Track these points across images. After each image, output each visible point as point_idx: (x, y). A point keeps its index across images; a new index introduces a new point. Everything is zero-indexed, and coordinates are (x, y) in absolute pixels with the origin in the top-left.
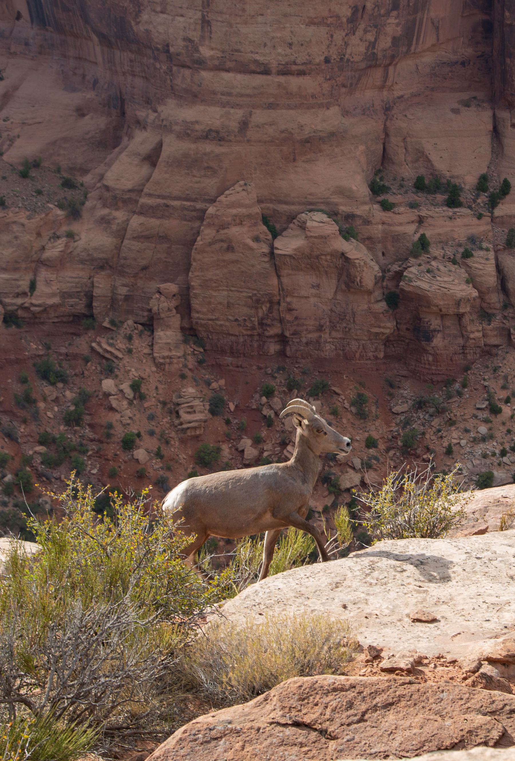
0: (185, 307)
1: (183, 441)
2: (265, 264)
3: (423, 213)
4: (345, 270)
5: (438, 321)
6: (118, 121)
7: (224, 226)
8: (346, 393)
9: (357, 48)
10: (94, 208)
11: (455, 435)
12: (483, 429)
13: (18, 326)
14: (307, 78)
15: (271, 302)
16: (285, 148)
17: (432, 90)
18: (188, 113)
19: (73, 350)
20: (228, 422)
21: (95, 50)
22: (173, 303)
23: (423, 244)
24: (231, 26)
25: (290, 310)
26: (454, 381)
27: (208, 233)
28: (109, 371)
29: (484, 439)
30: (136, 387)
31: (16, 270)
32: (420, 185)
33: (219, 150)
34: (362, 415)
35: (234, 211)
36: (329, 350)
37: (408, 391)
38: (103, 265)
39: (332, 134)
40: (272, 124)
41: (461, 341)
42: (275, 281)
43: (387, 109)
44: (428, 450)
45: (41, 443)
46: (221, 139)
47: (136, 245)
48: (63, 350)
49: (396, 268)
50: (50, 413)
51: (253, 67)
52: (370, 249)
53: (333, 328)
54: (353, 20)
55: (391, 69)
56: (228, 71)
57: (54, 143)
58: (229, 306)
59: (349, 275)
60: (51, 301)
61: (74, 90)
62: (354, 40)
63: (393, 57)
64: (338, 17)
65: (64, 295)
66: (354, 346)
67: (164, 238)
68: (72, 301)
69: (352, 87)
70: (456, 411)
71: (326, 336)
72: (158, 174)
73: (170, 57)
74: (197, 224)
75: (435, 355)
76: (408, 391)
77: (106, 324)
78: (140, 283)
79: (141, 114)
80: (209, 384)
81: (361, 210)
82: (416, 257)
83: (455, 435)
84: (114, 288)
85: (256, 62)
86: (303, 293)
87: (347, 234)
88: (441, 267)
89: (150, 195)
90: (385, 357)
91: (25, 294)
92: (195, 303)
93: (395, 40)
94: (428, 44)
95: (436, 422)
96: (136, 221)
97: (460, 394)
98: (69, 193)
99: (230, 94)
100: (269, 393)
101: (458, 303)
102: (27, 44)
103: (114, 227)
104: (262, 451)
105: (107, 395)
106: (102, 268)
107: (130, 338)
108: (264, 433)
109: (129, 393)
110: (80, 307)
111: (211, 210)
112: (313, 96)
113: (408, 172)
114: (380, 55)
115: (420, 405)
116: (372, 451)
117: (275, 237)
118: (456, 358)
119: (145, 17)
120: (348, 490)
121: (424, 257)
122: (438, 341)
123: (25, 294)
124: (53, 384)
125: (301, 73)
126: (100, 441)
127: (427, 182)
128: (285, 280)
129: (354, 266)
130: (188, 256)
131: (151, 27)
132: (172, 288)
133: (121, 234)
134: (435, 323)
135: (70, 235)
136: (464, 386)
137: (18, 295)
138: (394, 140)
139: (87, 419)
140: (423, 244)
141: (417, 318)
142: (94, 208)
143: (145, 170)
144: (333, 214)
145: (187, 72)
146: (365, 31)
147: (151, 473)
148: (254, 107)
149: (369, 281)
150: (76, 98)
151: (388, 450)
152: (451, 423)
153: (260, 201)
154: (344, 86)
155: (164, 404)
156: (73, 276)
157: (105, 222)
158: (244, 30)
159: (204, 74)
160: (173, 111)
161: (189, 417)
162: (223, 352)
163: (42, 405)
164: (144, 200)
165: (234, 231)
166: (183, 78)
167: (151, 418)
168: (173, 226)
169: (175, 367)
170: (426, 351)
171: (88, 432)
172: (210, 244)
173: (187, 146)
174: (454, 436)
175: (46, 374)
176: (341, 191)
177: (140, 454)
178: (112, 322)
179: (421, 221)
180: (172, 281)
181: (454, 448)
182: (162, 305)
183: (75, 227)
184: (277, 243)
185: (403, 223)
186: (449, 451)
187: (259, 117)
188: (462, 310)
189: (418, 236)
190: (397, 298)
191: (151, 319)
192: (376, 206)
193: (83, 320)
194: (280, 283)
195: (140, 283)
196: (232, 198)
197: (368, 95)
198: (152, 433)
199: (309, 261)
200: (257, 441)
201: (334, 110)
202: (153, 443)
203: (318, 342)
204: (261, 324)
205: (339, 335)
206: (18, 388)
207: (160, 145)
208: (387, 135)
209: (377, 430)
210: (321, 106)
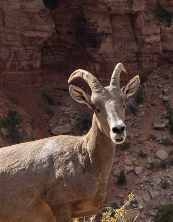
5: (107, 23)
12: (163, 153)
29: (164, 165)
41: (134, 47)
83: (128, 160)
90: (43, 66)
134: (103, 25)
141: (81, 20)
181: (128, 177)
188: (135, 9)
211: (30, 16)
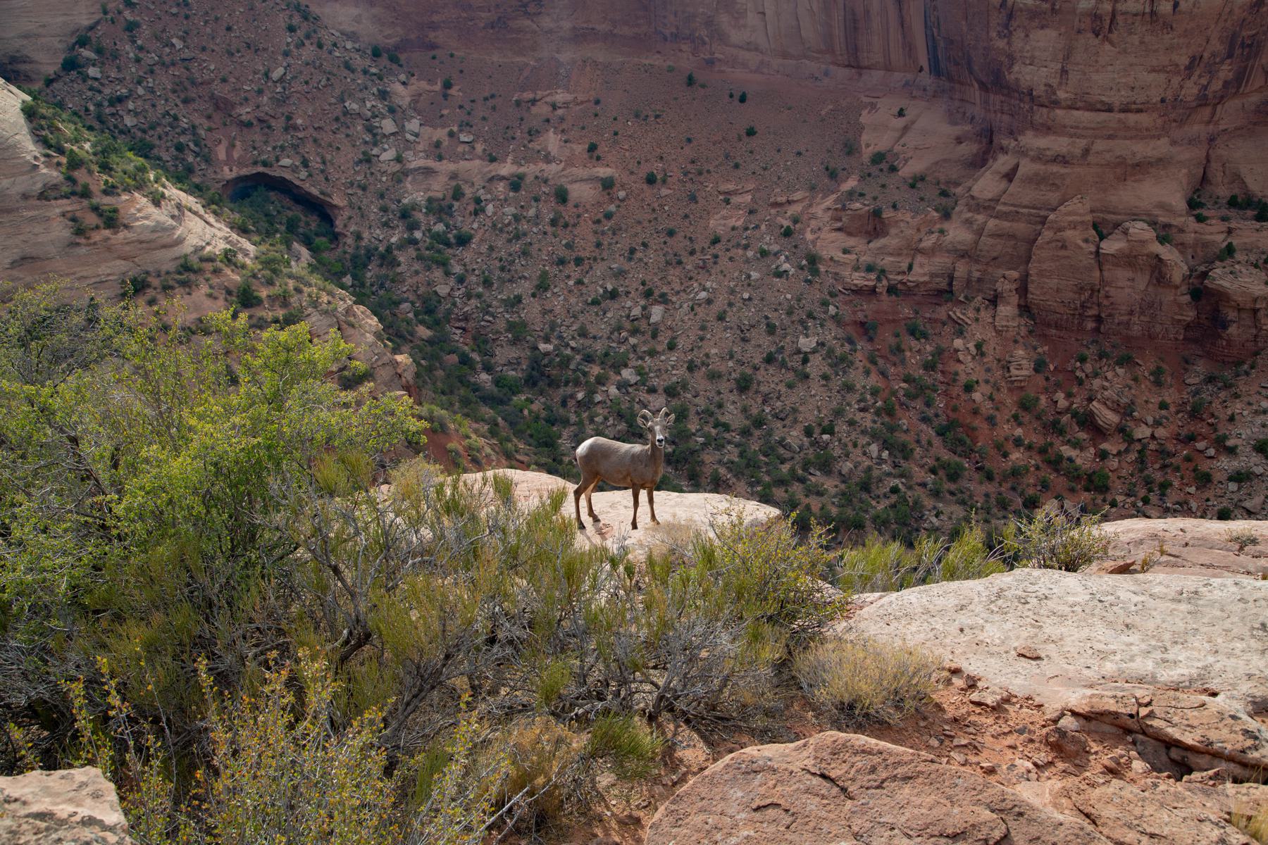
0: (1023, 290)
1: (1010, 390)
2: (1091, 260)
3: (1232, 226)
4: (1157, 268)
5: (1236, 314)
6: (988, 144)
7: (1060, 230)
8: (1147, 365)
9: (1191, 90)
10: (961, 212)
11: (1238, 406)
13: (897, 295)
14: (1144, 114)
15: (1092, 290)
16: (1118, 170)
17: (1255, 124)
18: (1042, 142)
19: (934, 316)
20: (1047, 379)
21: (975, 93)
22: (1014, 286)
23: (1230, 250)
24: (1085, 74)
25: (1107, 297)
26: (1244, 363)
27: (1047, 234)
28: (960, 333)
30: (978, 346)
31: (899, 255)
32: (1233, 203)
33: (1063, 171)
34: (1158, 383)
35: (1071, 218)
36: (1136, 330)
37: (1201, 368)
38: (964, 254)
39: (1160, 160)
40: (1109, 151)
41: (1254, 331)
42: (1097, 274)
43: (1211, 140)
44: (1213, 415)
45: (905, 381)
46: (1066, 162)
47: (991, 241)
48: (928, 315)
49: (1202, 268)
50: (913, 360)
51: (1099, 106)
52: (1181, 252)
53: (1142, 313)
54: (1190, 68)
55: (1219, 107)
56: (1077, 109)
57: (937, 163)
58: (1058, 290)
59: (1160, 272)
60: (922, 279)
61: (956, 124)
62: (1189, 84)
63: (1222, 97)
64: (1177, 65)
65: (933, 275)
66: (1158, 328)
67: (1012, 236)
68: (938, 280)
69: (1181, 122)
70: (1242, 386)
71: (1135, 319)
72: (1013, 188)
73: (1032, 99)
74: (1039, 227)
75: (1229, 341)
76: (1201, 368)
77: (961, 298)
78: (990, 270)
79: (1005, 142)
80: (1035, 349)
81: (1177, 221)
82: (1222, 261)
83: (1238, 406)
84: (970, 272)
85: (1102, 102)
86: (1120, 284)
87: (1162, 240)
88: (1244, 270)
89: (1005, 204)
91: (904, 273)
92: (1031, 287)
93: (1226, 84)
94: (1257, 85)
95: (1223, 395)
96: (992, 223)
97: (1247, 374)
98: (944, 201)
99: (1077, 127)
100: (1083, 360)
101: (1255, 300)
102: (925, 90)
103: (975, 227)
104: (1072, 403)
105: (957, 351)
106: (963, 257)
107: (978, 310)
108: (1075, 390)
109: (973, 351)
110: (944, 285)
111: (1052, 217)
112: (1147, 130)
113: (1223, 192)
114: (1210, 96)
115: (1210, 379)
116: (1164, 412)
117: (1101, 239)
118: (1248, 344)
119: (1016, 68)
120: (1139, 440)
121: (1229, 261)
122: (1233, 330)
123: (904, 273)
124: (918, 339)
125: (1139, 111)
126: (948, 384)
127: (1239, 200)
128: (1106, 274)
129: (1166, 265)
130: (1030, 250)
131: (1020, 76)
132: (1015, 274)
133: (980, 232)
134: (1232, 315)
135: (942, 232)
136: (1252, 367)
137: (899, 273)
138: (1213, 165)
139: (940, 367)
140: (1230, 250)
141: (1216, 310)
142: (961, 212)
143: (1004, 184)
144: (1153, 224)
145: (1045, 110)
146: (1200, 76)
147: (983, 410)
148: (1096, 137)
149: (1177, 277)
150: (957, 130)
151: (1178, 412)
152: (1236, 396)
153: (1092, 211)
154: (1175, 121)
155: (999, 360)
156: (940, 262)
157: (968, 222)
158: (1095, 77)
159: (1058, 112)
160: (1031, 140)
161: (1017, 372)
162: (1049, 325)
163: (908, 354)
164: (999, 208)
165: (1069, 234)
166: (1041, 115)
167: (988, 370)
168: (1021, 228)
169: (1011, 334)
170: (1222, 338)
171: (939, 376)
172: (1048, 243)
173: (1038, 167)
174: (1237, 407)
175: (913, 332)
176: (1162, 206)
177: (977, 396)
178: (966, 297)
179: (1230, 231)
180: (1014, 269)
181: (1237, 417)
182: (1005, 287)
183: (946, 226)
184: (1103, 245)
185: (1214, 233)
186: (1232, 419)
187: (1100, 145)
188: (1258, 306)
189: (1225, 244)
190: (1201, 293)
191: (996, 297)
192: (1192, 219)
193: (944, 293)
194: (1102, 275)
195: (990, 270)
196: (1070, 208)
197: (1196, 129)
198: (987, 382)
199: (1128, 260)
200: (1069, 395)
201: (1165, 140)
202: (986, 389)
203: (1128, 323)
204: (1082, 306)
205: (1146, 319)
206: (892, 341)
207: (1017, 166)
208: (1208, 161)
209: (1170, 396)
210: (1153, 137)
211: (1180, 306)
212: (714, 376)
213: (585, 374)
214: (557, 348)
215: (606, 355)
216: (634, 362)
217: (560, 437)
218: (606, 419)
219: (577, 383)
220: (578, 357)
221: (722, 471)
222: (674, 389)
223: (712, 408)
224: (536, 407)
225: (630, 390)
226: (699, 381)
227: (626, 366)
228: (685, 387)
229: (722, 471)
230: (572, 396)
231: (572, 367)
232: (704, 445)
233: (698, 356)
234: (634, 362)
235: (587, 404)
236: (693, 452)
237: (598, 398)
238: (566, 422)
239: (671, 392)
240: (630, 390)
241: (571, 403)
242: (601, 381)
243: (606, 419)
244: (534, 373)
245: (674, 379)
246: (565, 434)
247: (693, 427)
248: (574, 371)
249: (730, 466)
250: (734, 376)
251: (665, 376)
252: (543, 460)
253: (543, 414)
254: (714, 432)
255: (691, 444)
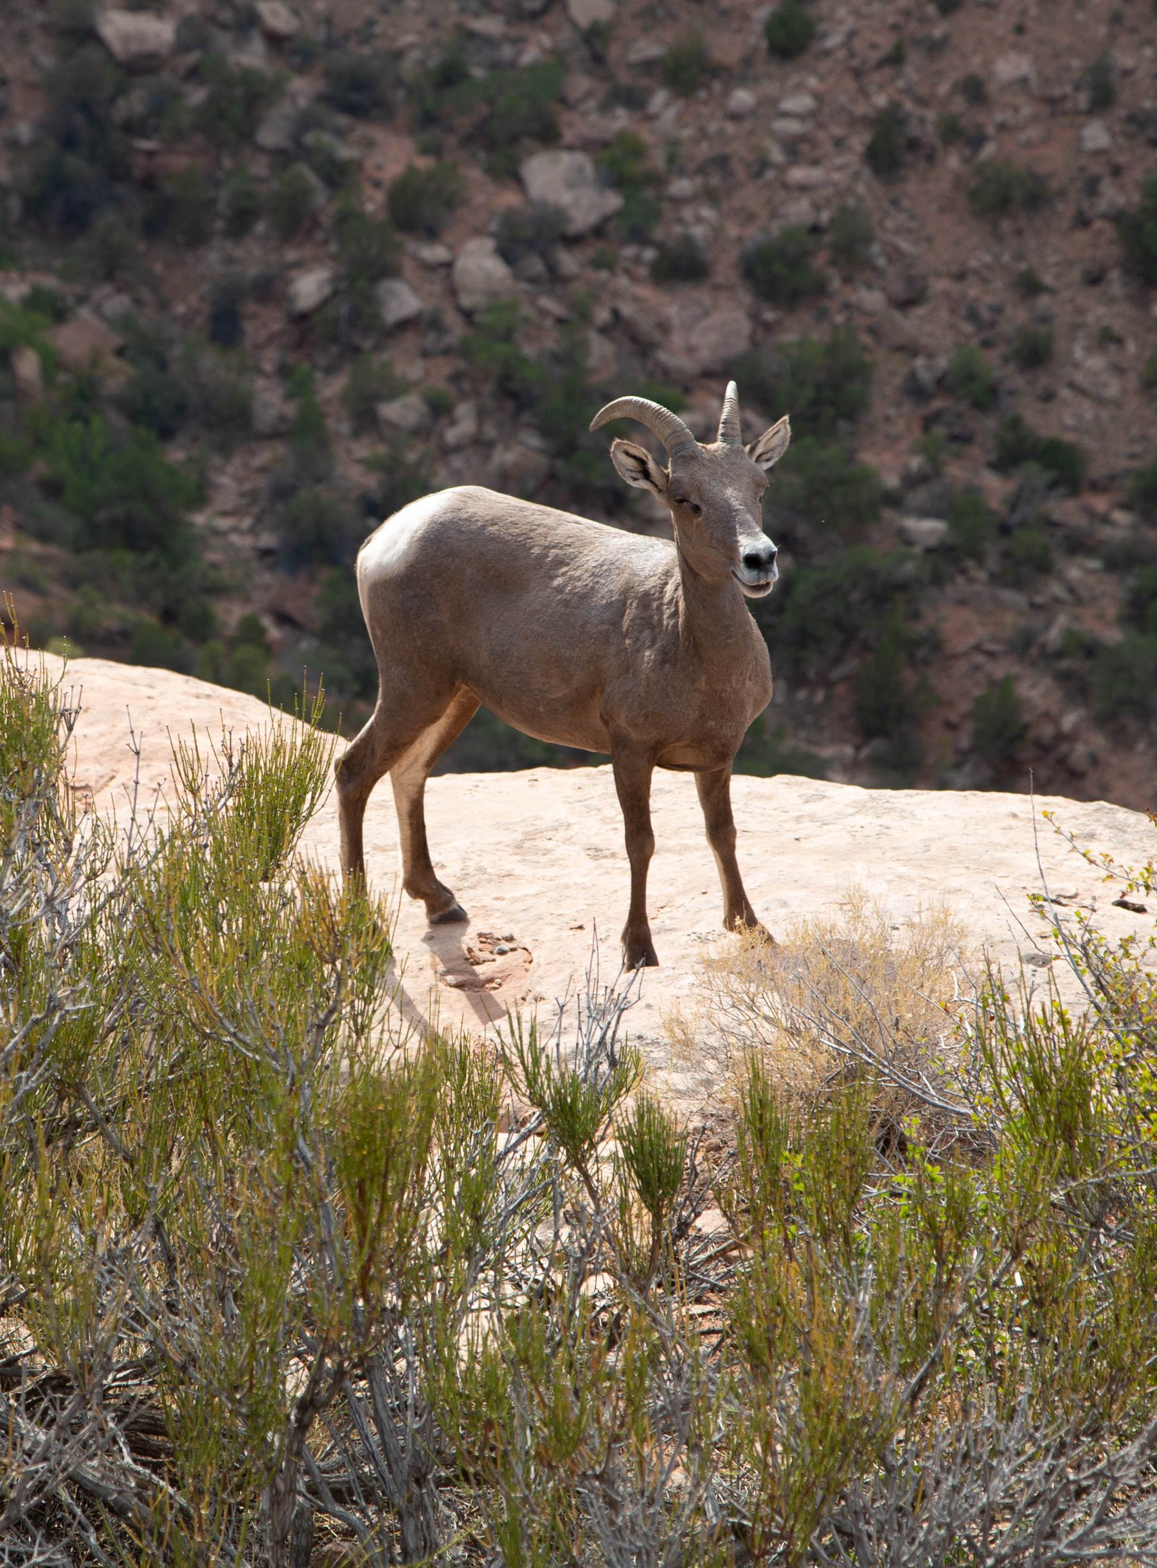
212: (1005, 200)
213: (337, 175)
214: (193, 35)
215: (450, 76)
216: (592, 121)
217: (200, 497)
218: (440, 409)
219: (294, 222)
220: (303, 88)
221: (1036, 692)
222: (798, 261)
223: (993, 364)
224: (78, 338)
225: (569, 261)
226: (923, 223)
227: (549, 137)
228: (850, 247)
229: (1036, 692)
230: (270, 289)
231: (271, 134)
232: (947, 558)
233: (923, 93)
234: (592, 121)
235: (341, 332)
236: (885, 593)
237: (402, 300)
238: (232, 423)
239: (778, 277)
240: (569, 261)
241: (262, 325)
242: (419, 211)
243: (440, 409)
244: (75, 163)
245: (799, 210)
246: (230, 480)
247: (887, 462)
248: (282, 158)
249: (1079, 667)
250: (1112, 196)
251: (749, 196)
252: (113, 615)
253: (117, 377)
254: (996, 488)
255: (878, 552)
